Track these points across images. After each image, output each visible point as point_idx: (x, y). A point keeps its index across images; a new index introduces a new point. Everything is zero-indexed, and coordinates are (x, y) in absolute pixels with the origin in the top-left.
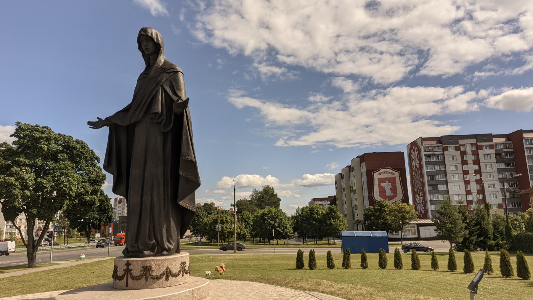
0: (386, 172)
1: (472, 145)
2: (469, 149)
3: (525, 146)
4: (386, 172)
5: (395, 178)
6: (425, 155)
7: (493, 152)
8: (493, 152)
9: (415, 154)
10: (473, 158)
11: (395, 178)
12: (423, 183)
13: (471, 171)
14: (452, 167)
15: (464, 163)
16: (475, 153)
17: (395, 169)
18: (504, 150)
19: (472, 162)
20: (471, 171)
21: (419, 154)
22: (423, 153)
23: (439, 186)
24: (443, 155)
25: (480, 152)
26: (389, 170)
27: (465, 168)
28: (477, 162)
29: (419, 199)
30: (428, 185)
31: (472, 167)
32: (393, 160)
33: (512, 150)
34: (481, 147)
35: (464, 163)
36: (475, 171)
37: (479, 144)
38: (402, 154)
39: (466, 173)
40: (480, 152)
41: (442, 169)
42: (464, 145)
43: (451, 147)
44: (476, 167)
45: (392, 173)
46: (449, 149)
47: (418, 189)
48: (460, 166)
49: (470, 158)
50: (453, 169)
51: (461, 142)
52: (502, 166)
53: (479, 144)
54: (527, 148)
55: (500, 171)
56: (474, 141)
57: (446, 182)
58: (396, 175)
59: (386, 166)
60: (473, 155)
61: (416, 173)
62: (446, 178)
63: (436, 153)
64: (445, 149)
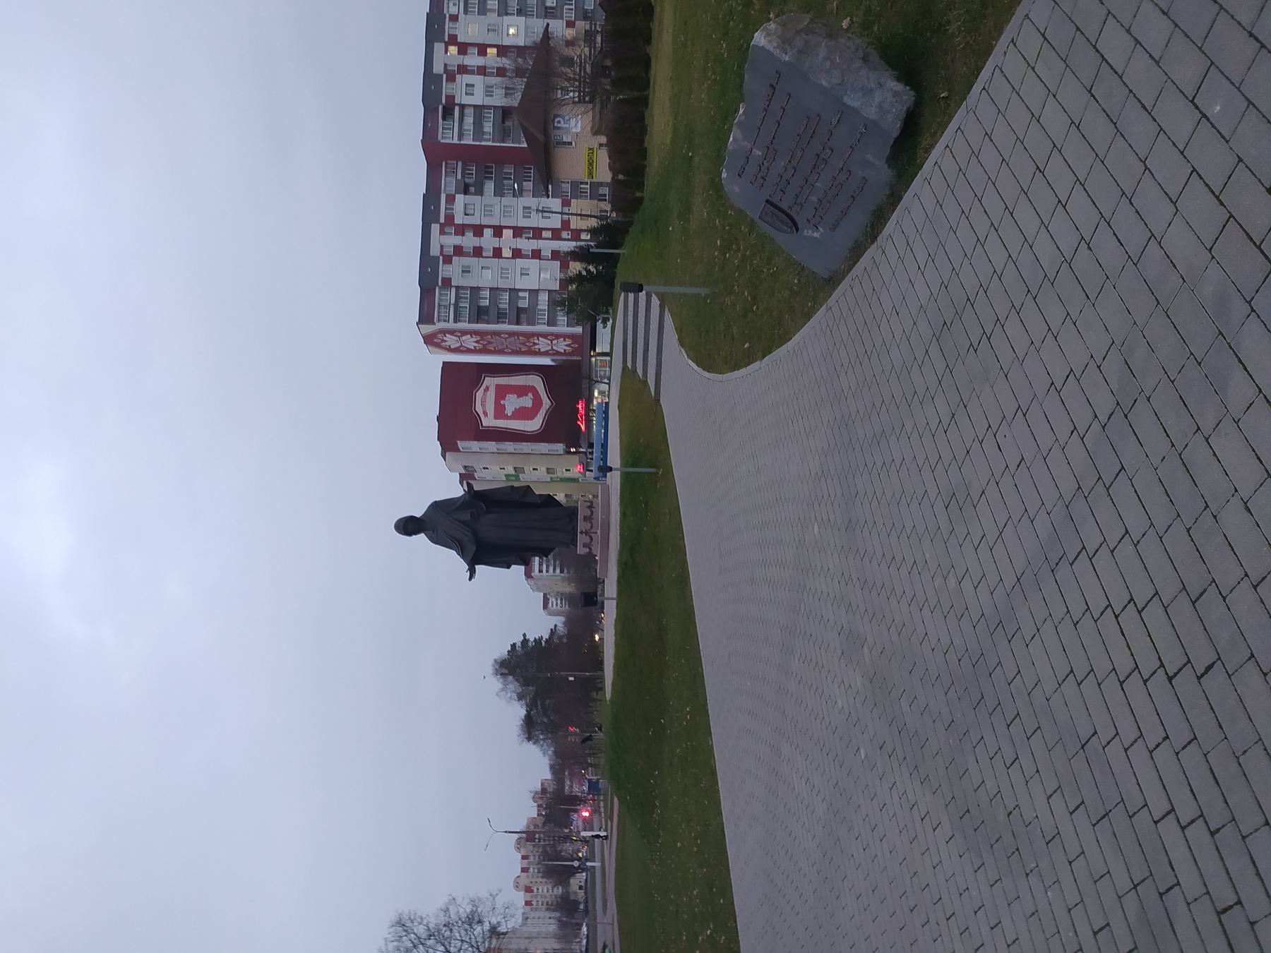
0: (483, 405)
1: (442, 232)
2: (451, 240)
3: (456, 141)
4: (483, 405)
5: (497, 386)
6: (455, 321)
7: (460, 198)
8: (460, 198)
9: (451, 341)
10: (470, 234)
11: (497, 386)
12: (512, 334)
13: (496, 242)
14: (485, 275)
15: (478, 252)
16: (461, 230)
17: (477, 383)
18: (459, 177)
19: (477, 239)
20: (496, 242)
21: (452, 332)
22: (451, 325)
23: (520, 305)
24: (457, 288)
25: (458, 220)
26: (479, 394)
27: (507, 253)
28: (478, 230)
29: (543, 344)
30: (518, 323)
31: (547, 246)
32: (458, 386)
33: (460, 164)
34: (450, 219)
35: (478, 252)
36: (495, 235)
37: (442, 220)
38: (447, 367)
39: (497, 253)
40: (458, 220)
41: (487, 294)
42: (442, 247)
43: (444, 271)
44: (488, 232)
45: (487, 389)
46: (446, 275)
47: (524, 344)
48: (482, 261)
49: (469, 241)
50: (488, 274)
51: (435, 251)
52: (489, 186)
53: (442, 220)
54: (460, 138)
55: (499, 192)
56: (435, 228)
57: (514, 292)
58: (490, 382)
59: (471, 401)
60: (463, 235)
61: (489, 343)
62: (505, 290)
63: (453, 301)
64: (447, 282)
